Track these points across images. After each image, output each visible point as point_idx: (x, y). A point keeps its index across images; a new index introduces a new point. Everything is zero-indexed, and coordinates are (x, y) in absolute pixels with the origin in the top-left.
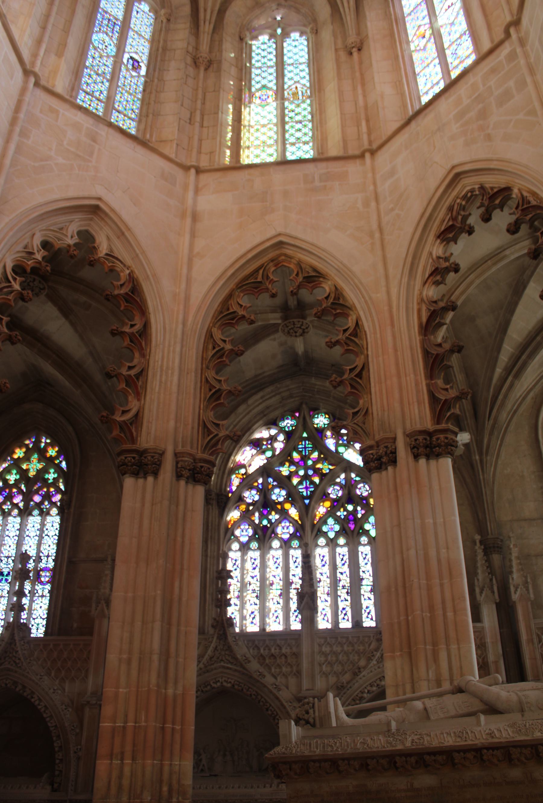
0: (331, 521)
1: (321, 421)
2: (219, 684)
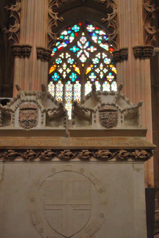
0: (93, 74)
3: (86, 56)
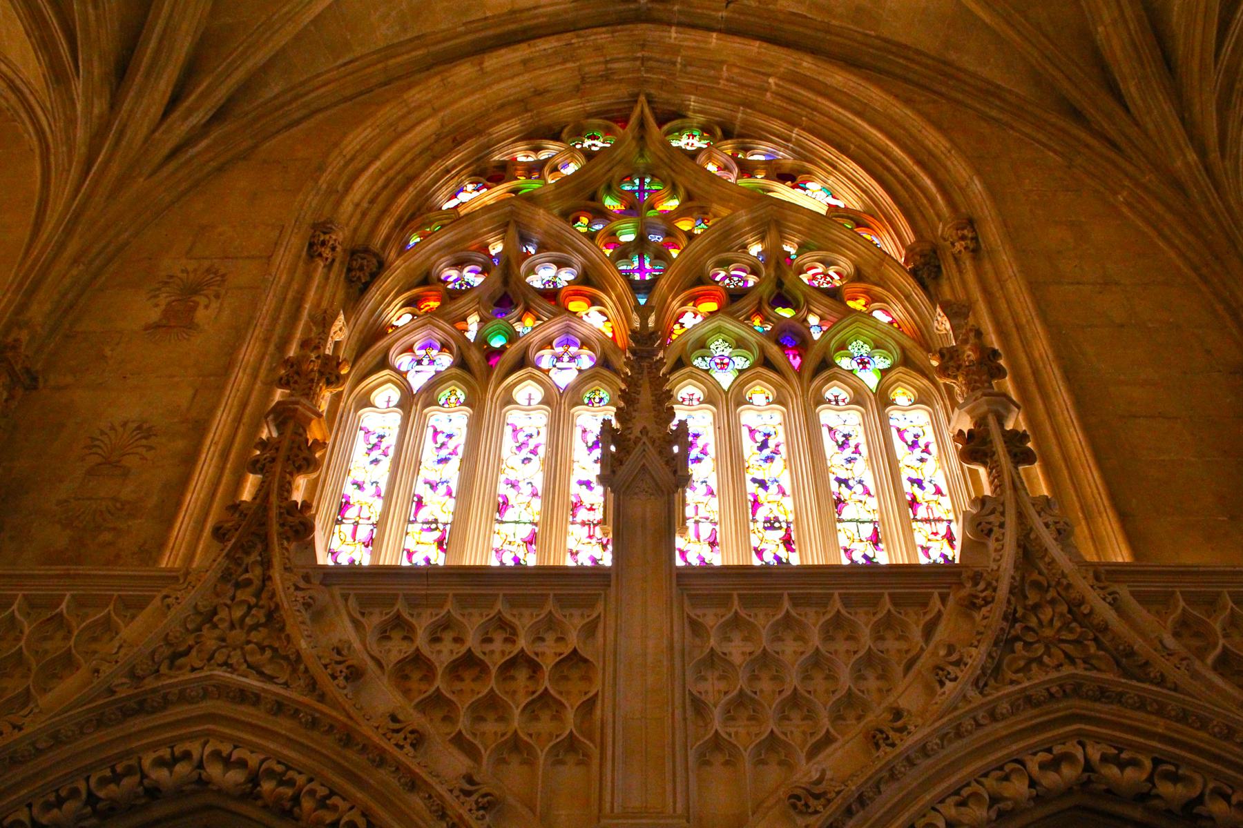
0: (719, 347)
1: (688, 142)
2: (182, 769)
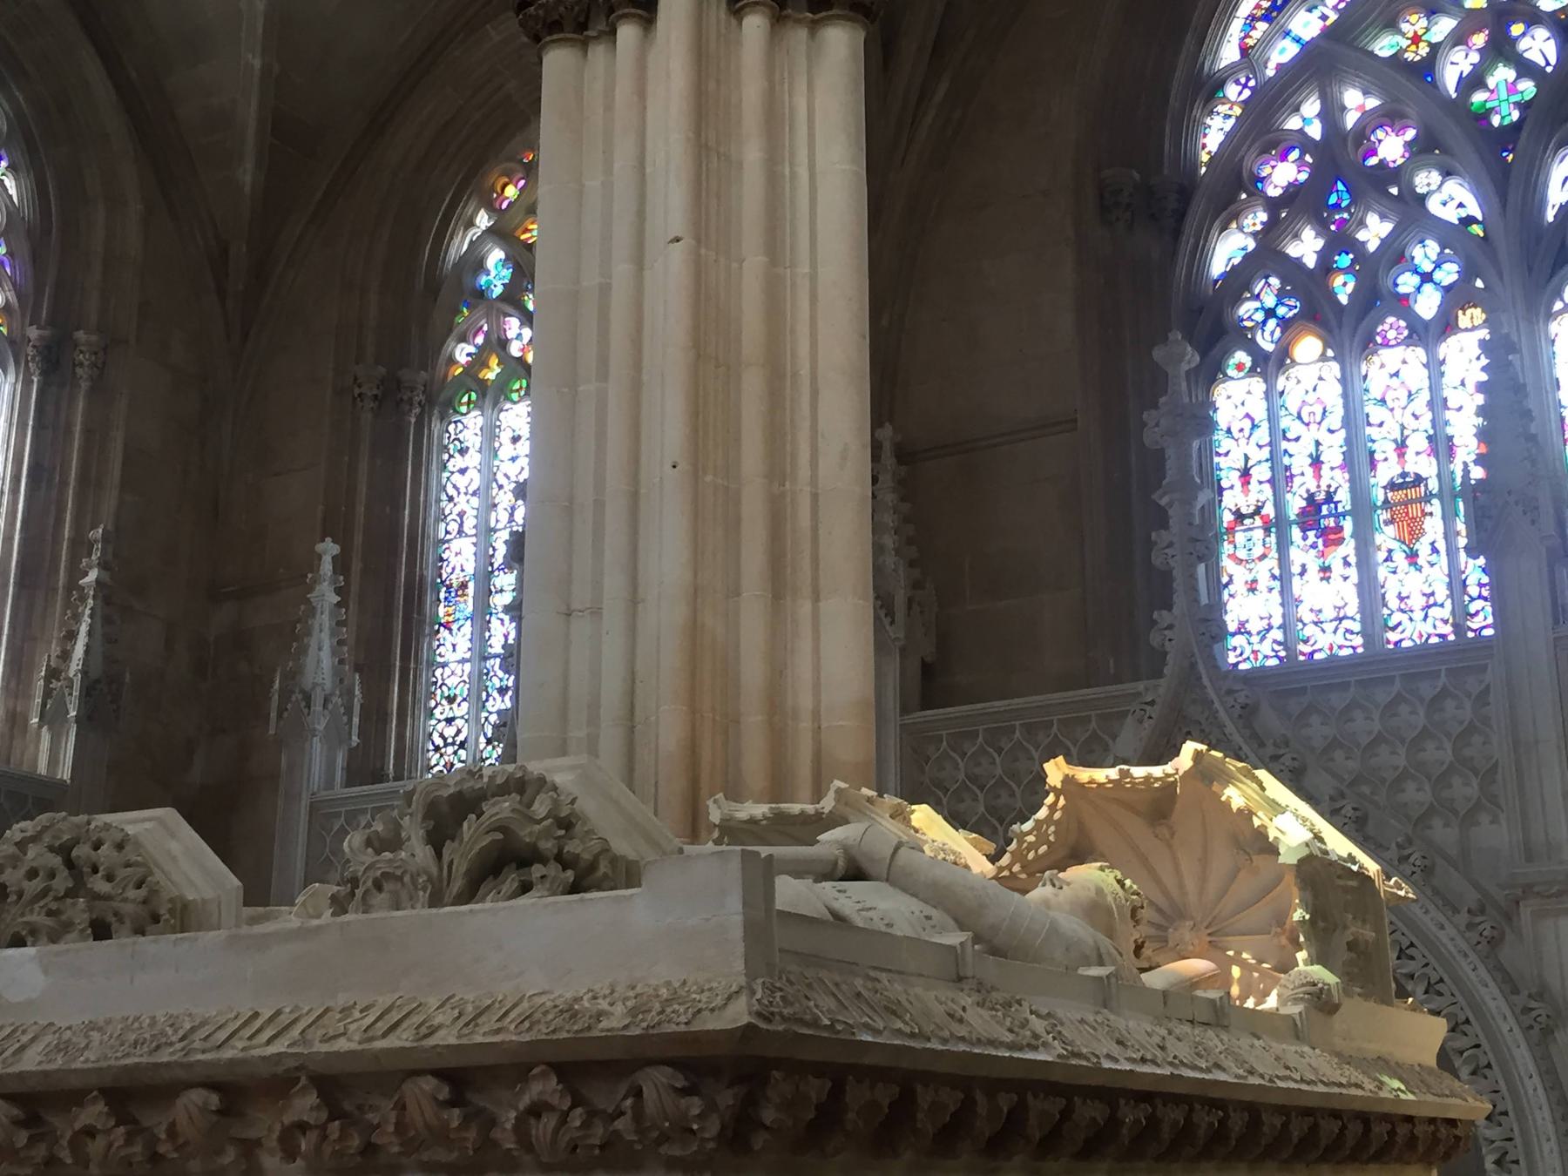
3: (1526, 69)
